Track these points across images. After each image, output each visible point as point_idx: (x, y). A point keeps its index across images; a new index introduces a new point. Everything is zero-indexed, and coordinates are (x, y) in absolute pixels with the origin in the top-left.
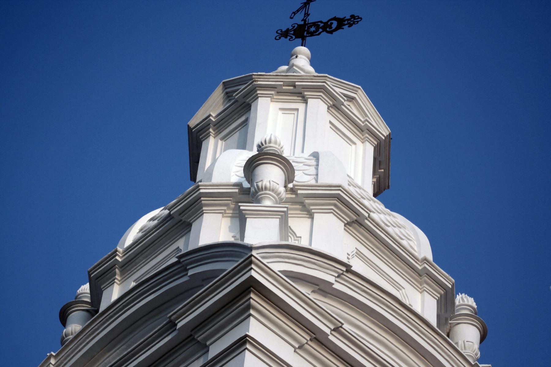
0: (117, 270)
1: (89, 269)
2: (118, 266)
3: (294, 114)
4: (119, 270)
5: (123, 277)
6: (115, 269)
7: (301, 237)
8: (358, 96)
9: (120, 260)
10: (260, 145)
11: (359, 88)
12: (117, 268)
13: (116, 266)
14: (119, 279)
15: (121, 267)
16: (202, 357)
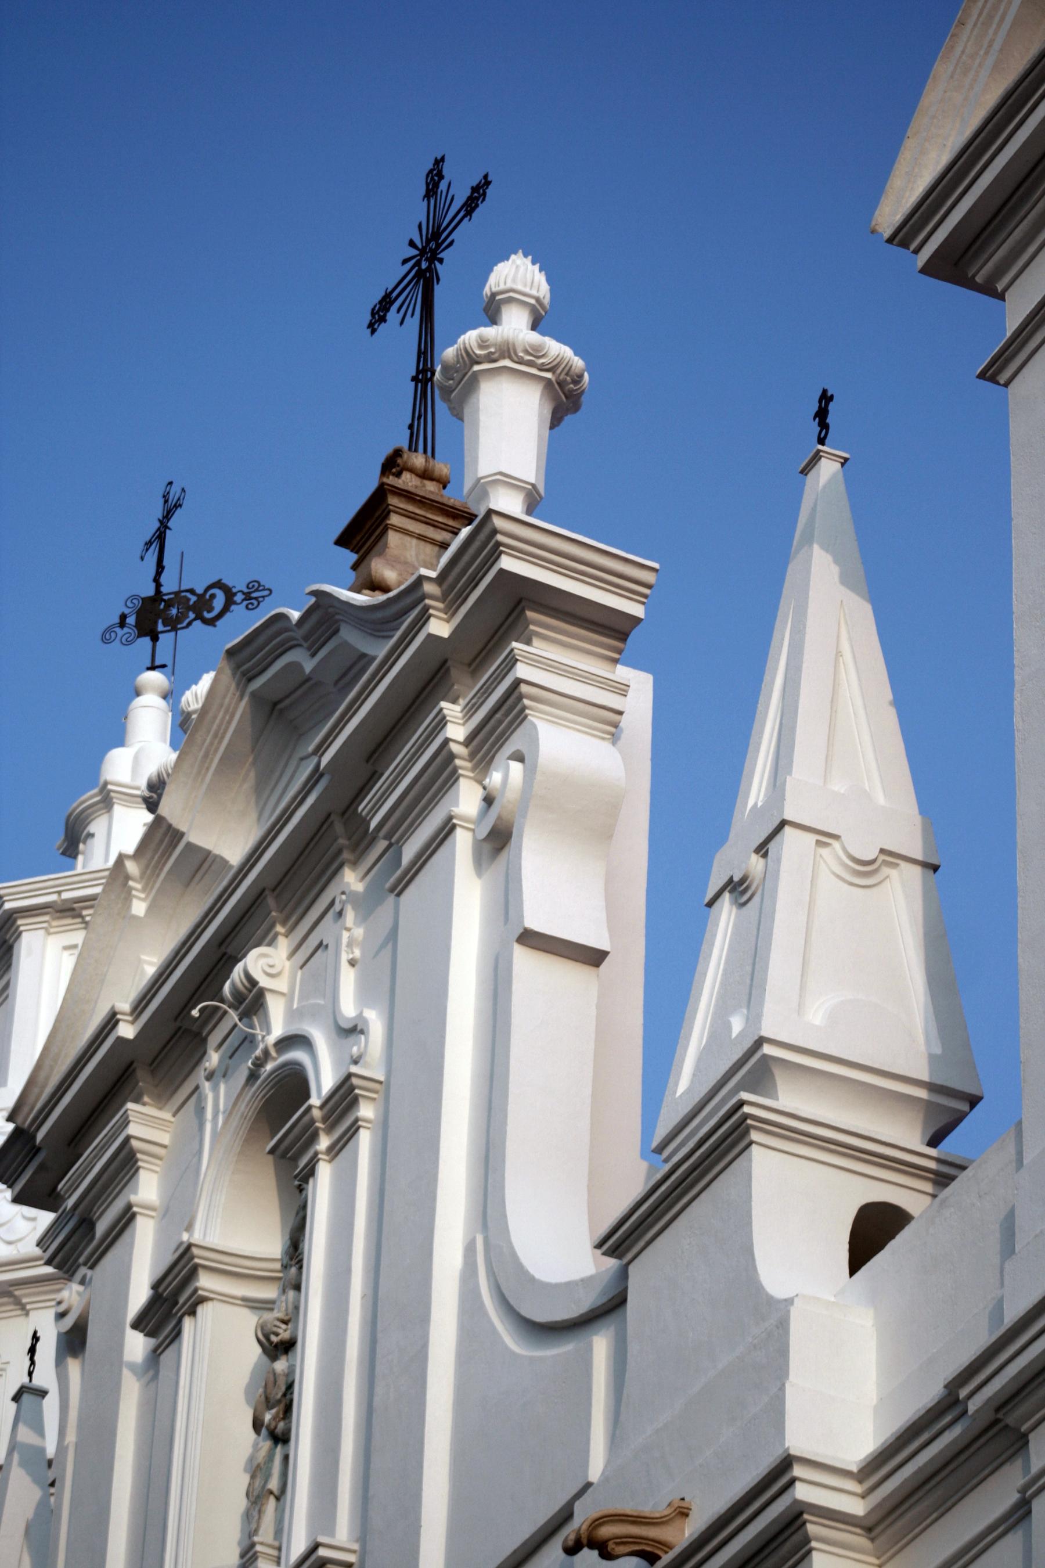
7: (8, 1363)
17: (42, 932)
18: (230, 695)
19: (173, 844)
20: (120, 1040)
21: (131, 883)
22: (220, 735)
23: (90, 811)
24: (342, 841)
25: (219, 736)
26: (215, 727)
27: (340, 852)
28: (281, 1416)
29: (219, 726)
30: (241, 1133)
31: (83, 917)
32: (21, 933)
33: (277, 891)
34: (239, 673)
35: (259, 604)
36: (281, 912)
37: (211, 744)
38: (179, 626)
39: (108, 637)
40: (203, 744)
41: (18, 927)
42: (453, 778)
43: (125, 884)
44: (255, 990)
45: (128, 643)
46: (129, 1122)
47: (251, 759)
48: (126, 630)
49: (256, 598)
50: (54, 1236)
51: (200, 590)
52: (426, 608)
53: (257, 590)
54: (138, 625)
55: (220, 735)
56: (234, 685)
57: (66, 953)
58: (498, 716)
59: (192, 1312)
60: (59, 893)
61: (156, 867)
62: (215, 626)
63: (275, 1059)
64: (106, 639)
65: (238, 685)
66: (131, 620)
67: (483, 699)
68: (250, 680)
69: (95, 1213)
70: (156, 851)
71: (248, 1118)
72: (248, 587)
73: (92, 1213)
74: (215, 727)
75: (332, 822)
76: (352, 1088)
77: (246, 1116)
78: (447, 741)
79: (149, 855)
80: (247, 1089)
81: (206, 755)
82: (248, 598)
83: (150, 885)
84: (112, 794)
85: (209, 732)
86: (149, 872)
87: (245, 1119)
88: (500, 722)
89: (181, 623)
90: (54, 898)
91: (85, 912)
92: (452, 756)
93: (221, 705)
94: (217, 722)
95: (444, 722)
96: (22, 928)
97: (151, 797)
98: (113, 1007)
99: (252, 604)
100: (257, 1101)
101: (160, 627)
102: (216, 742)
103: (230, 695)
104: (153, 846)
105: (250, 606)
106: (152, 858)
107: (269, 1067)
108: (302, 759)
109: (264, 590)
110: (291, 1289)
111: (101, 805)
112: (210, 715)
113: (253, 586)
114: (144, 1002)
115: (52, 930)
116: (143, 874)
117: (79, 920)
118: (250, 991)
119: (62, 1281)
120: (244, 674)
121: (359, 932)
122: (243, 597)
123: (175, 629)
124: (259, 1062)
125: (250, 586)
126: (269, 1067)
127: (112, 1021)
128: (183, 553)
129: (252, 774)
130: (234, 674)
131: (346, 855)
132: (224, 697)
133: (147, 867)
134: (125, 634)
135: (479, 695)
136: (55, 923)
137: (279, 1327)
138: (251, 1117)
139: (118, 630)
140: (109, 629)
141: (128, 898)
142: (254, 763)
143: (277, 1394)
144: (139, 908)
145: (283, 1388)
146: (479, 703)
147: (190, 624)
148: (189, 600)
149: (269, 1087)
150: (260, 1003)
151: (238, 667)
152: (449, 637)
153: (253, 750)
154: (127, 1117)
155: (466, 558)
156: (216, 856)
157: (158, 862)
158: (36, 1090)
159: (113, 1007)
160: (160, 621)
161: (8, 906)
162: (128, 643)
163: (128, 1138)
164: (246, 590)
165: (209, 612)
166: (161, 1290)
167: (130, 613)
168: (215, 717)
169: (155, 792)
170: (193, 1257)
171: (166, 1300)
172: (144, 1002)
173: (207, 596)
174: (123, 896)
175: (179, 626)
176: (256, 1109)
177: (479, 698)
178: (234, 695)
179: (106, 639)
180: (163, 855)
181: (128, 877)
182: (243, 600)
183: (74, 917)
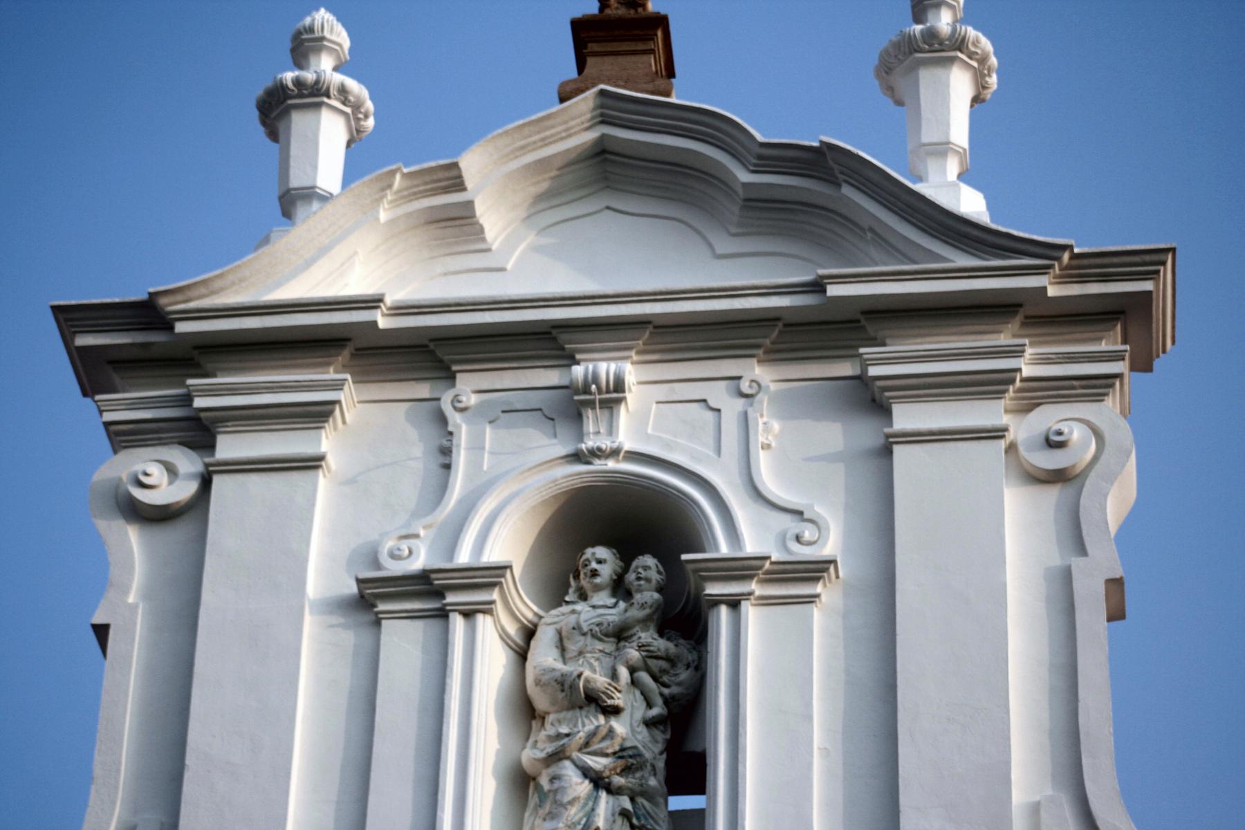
18: (578, 121)
19: (448, 190)
20: (374, 324)
21: (388, 192)
22: (546, 142)
24: (768, 341)
25: (545, 142)
26: (548, 133)
27: (758, 346)
28: (618, 771)
29: (552, 136)
30: (544, 493)
33: (658, 330)
34: (599, 111)
36: (644, 344)
37: (535, 142)
40: (526, 138)
42: (999, 394)
43: (383, 190)
44: (615, 395)
46: (341, 389)
47: (554, 173)
50: (132, 407)
52: (1050, 267)
55: (546, 142)
56: (589, 116)
58: (1075, 383)
59: (468, 615)
61: (415, 194)
63: (618, 461)
65: (593, 118)
67: (1062, 361)
68: (602, 122)
69: (227, 426)
70: (426, 183)
71: (559, 487)
73: (220, 425)
74: (548, 133)
75: (776, 326)
76: (826, 570)
77: (560, 484)
78: (1020, 370)
79: (415, 182)
80: (562, 461)
81: (522, 148)
83: (399, 202)
85: (539, 132)
86: (406, 193)
87: (556, 485)
88: (1073, 388)
92: (1013, 381)
93: (566, 122)
94: (553, 131)
95: (1020, 354)
97: (293, 91)
98: (383, 295)
100: (579, 480)
102: (540, 144)
103: (578, 121)
104: (427, 178)
106: (418, 186)
107: (611, 464)
108: (608, 208)
110: (625, 666)
112: (551, 122)
114: (416, 310)
116: (399, 191)
118: (608, 392)
120: (602, 115)
121: (776, 426)
124: (599, 453)
126: (611, 464)
127: (373, 302)
129: (545, 186)
130: (594, 109)
131: (760, 352)
132: (573, 119)
133: (407, 189)
135: (1061, 356)
137: (613, 693)
138: (564, 487)
141: (379, 200)
142: (552, 178)
143: (607, 748)
144: (383, 216)
145: (617, 748)
146: (1055, 361)
149: (603, 479)
150: (612, 405)
151: (602, 106)
152: (1051, 297)
153: (559, 169)
154: (343, 385)
155: (1115, 260)
156: (477, 223)
157: (420, 192)
158: (203, 290)
159: (383, 295)
163: (338, 402)
166: (433, 576)
168: (553, 127)
169: (299, 90)
170: (503, 576)
171: (431, 584)
172: (416, 310)
174: (377, 197)
176: (572, 485)
177: (1059, 358)
178: (583, 123)
180: (432, 189)
181: (390, 186)
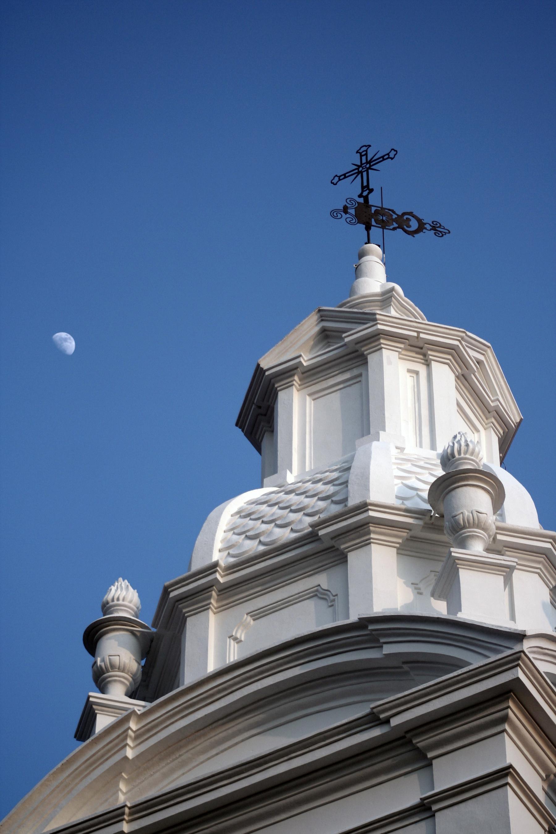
0: (214, 593)
1: (167, 583)
2: (216, 588)
3: (413, 377)
4: (216, 594)
5: (220, 604)
6: (212, 591)
8: (486, 358)
9: (221, 580)
10: (450, 457)
11: (488, 347)
12: (214, 590)
13: (214, 587)
14: (215, 605)
15: (219, 591)
16: (417, 772)
17: (397, 353)
23: (366, 304)
31: (425, 355)
32: (381, 348)
35: (443, 235)
38: (387, 227)
39: (335, 214)
41: (380, 344)
45: (350, 223)
48: (348, 216)
49: (441, 232)
51: (400, 213)
53: (439, 227)
54: (356, 216)
57: (408, 375)
60: (418, 333)
62: (414, 237)
64: (333, 214)
66: (352, 211)
72: (433, 222)
82: (434, 229)
84: (393, 299)
89: (389, 226)
90: (415, 334)
91: (430, 352)
96: (383, 346)
99: (439, 234)
101: (373, 223)
105: (437, 234)
109: (444, 229)
111: (379, 303)
113: (436, 224)
115: (401, 356)
117: (421, 357)
119: (544, 556)
122: (431, 227)
123: (383, 228)
125: (435, 223)
128: (381, 188)
134: (352, 218)
136: (403, 352)
139: (342, 213)
140: (337, 211)
147: (394, 229)
148: (392, 215)
160: (373, 220)
161: (380, 327)
162: (350, 223)
164: (432, 225)
165: (407, 227)
167: (350, 207)
173: (405, 217)
175: (387, 227)
179: (333, 214)
182: (431, 230)
183: (417, 353)
